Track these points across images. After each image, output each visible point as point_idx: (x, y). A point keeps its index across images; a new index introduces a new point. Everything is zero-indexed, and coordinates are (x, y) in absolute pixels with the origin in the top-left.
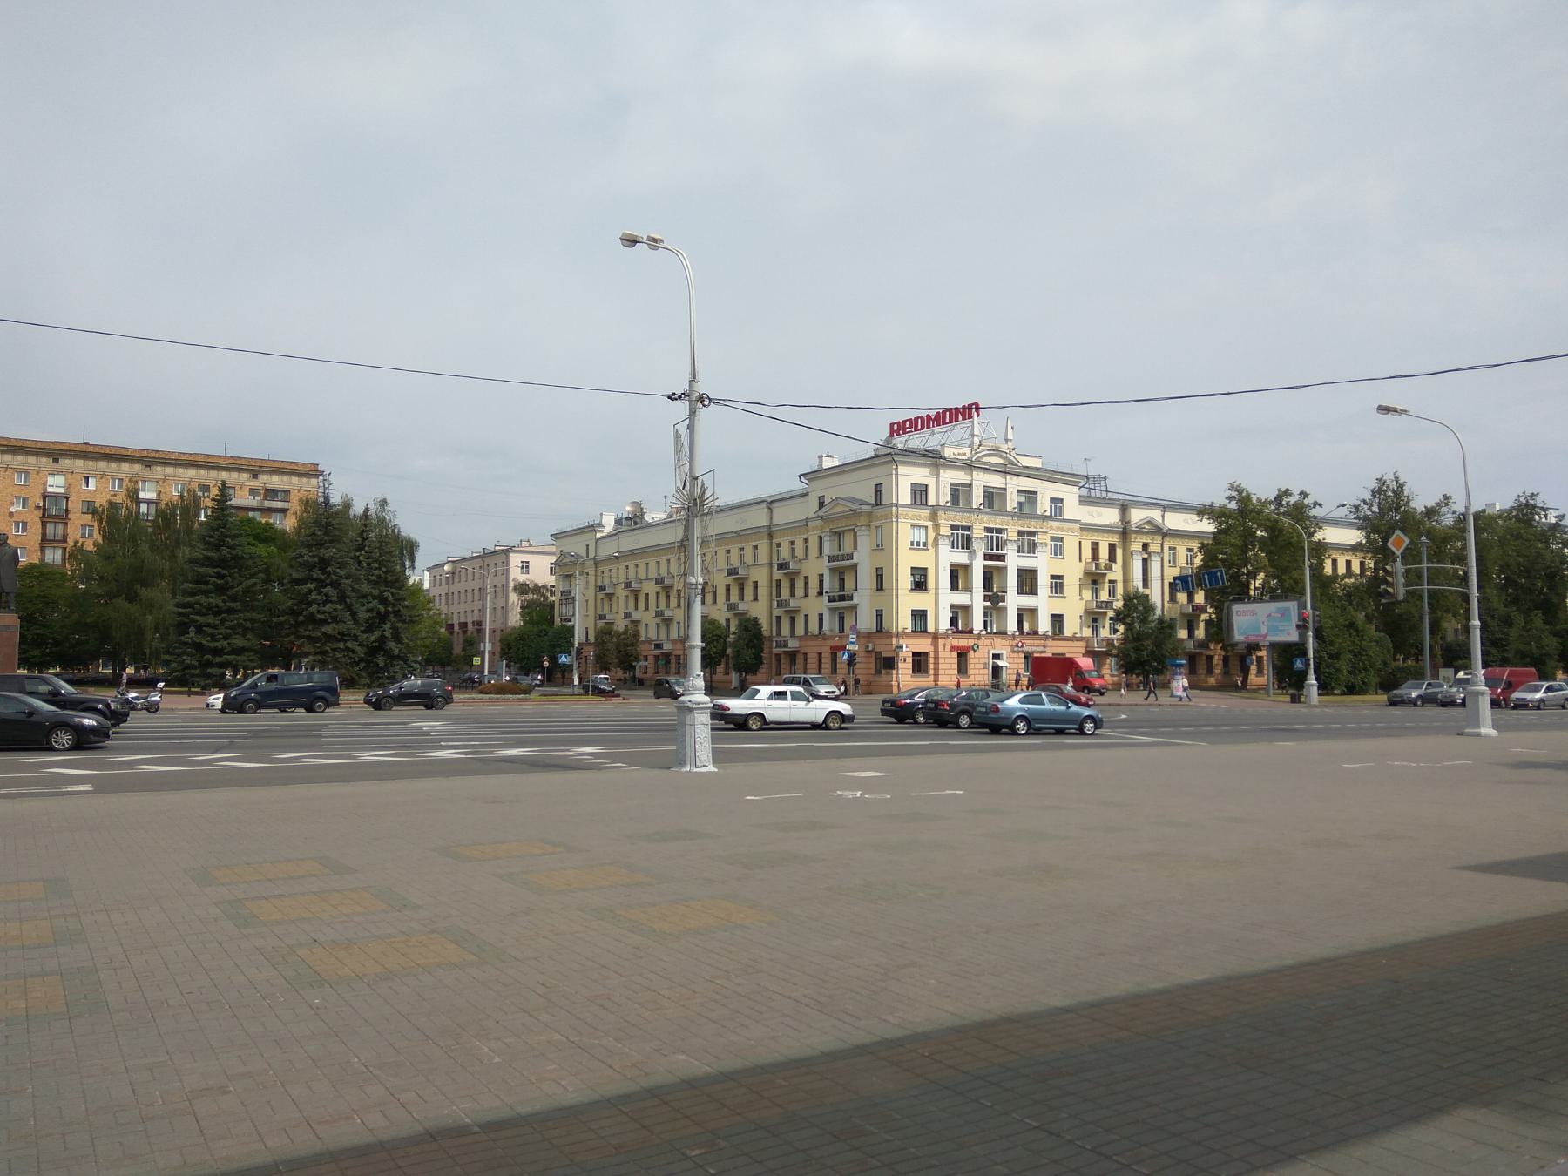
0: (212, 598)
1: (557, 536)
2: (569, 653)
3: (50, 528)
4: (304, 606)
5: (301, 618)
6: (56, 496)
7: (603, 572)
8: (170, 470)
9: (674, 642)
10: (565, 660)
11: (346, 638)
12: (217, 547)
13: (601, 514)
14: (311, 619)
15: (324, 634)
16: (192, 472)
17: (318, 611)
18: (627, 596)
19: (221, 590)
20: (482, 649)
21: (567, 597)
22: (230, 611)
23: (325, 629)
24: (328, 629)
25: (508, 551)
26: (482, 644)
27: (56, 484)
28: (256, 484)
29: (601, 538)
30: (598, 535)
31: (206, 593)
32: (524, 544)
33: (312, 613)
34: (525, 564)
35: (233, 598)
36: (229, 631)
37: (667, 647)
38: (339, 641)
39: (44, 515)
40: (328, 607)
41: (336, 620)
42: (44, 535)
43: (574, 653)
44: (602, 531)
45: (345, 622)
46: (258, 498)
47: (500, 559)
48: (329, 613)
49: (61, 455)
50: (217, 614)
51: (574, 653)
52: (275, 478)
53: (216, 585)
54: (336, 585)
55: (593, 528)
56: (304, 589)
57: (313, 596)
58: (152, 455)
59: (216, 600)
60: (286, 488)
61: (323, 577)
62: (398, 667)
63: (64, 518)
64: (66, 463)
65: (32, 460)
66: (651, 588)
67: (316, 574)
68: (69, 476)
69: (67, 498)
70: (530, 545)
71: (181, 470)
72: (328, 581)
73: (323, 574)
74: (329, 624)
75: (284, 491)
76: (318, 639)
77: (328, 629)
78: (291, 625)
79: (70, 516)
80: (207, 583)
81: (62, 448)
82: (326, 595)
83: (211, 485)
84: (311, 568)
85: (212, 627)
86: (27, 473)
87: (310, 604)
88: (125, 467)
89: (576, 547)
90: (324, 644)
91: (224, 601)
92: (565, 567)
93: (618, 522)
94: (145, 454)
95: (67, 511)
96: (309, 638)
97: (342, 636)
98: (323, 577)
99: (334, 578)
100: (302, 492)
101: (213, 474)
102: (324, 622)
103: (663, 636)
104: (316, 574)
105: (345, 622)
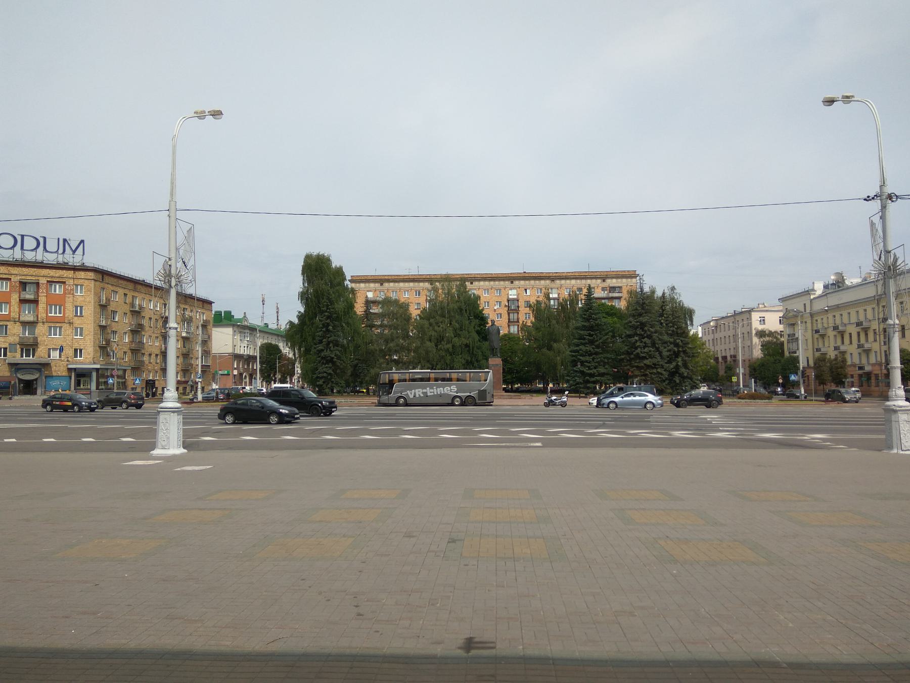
0: (587, 347)
1: (783, 300)
2: (797, 374)
3: (511, 315)
4: (633, 349)
5: (632, 356)
6: (513, 300)
7: (817, 320)
8: (563, 282)
9: (873, 365)
10: (794, 378)
11: (657, 367)
12: (588, 320)
13: (813, 283)
14: (638, 357)
15: (645, 364)
16: (573, 282)
17: (641, 352)
18: (835, 336)
19: (592, 342)
20: (738, 372)
21: (793, 338)
22: (596, 354)
23: (646, 362)
24: (647, 362)
25: (750, 312)
26: (738, 369)
27: (513, 294)
28: (605, 285)
29: (814, 298)
30: (812, 297)
31: (584, 344)
32: (760, 306)
33: (638, 353)
34: (762, 319)
35: (598, 347)
36: (597, 364)
37: (868, 368)
38: (653, 368)
39: (508, 309)
40: (646, 350)
41: (651, 357)
42: (509, 319)
43: (800, 373)
44: (815, 294)
45: (656, 358)
46: (606, 292)
47: (745, 316)
48: (647, 353)
49: (514, 279)
50: (590, 355)
51: (800, 373)
52: (614, 280)
53: (589, 339)
54: (649, 337)
55: (807, 293)
56: (633, 340)
57: (638, 344)
58: (554, 275)
59: (589, 348)
60: (620, 285)
61: (643, 333)
62: (688, 383)
63: (517, 311)
64: (516, 283)
65: (502, 283)
66: (853, 330)
67: (639, 331)
68: (518, 289)
69: (518, 301)
70: (765, 307)
71: (568, 281)
72: (645, 335)
73: (643, 331)
74: (647, 359)
75: (619, 287)
76: (642, 368)
77: (647, 362)
78: (628, 360)
79: (519, 309)
80: (584, 339)
81: (514, 276)
82: (645, 343)
83: (583, 288)
84: (636, 328)
85: (587, 362)
86: (500, 290)
87: (636, 348)
88: (543, 282)
89: (797, 305)
90: (645, 370)
91: (593, 348)
92: (789, 319)
93: (826, 287)
94: (551, 275)
95: (518, 307)
96: (637, 367)
97: (655, 366)
98: (643, 333)
99: (649, 333)
100: (628, 287)
101: (584, 281)
102: (645, 358)
103: (864, 361)
104: (639, 331)
105: (656, 358)
